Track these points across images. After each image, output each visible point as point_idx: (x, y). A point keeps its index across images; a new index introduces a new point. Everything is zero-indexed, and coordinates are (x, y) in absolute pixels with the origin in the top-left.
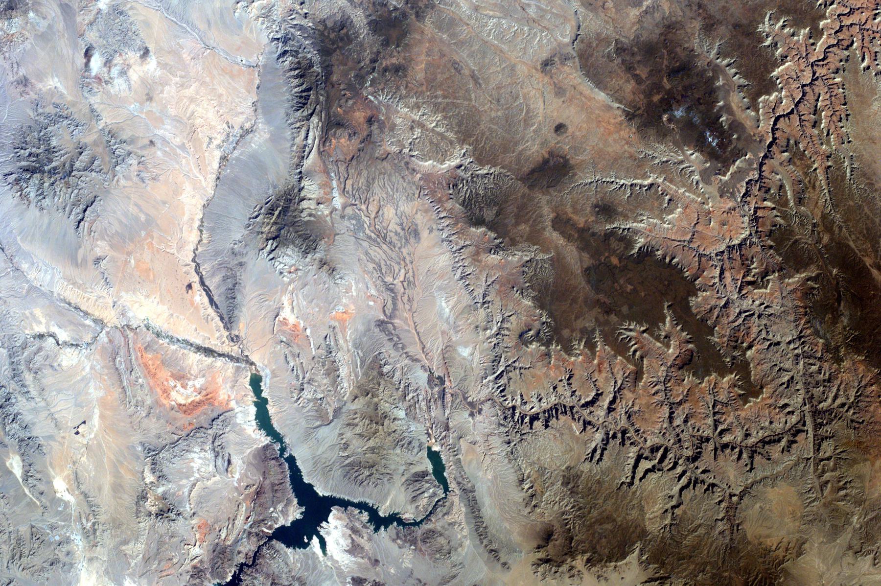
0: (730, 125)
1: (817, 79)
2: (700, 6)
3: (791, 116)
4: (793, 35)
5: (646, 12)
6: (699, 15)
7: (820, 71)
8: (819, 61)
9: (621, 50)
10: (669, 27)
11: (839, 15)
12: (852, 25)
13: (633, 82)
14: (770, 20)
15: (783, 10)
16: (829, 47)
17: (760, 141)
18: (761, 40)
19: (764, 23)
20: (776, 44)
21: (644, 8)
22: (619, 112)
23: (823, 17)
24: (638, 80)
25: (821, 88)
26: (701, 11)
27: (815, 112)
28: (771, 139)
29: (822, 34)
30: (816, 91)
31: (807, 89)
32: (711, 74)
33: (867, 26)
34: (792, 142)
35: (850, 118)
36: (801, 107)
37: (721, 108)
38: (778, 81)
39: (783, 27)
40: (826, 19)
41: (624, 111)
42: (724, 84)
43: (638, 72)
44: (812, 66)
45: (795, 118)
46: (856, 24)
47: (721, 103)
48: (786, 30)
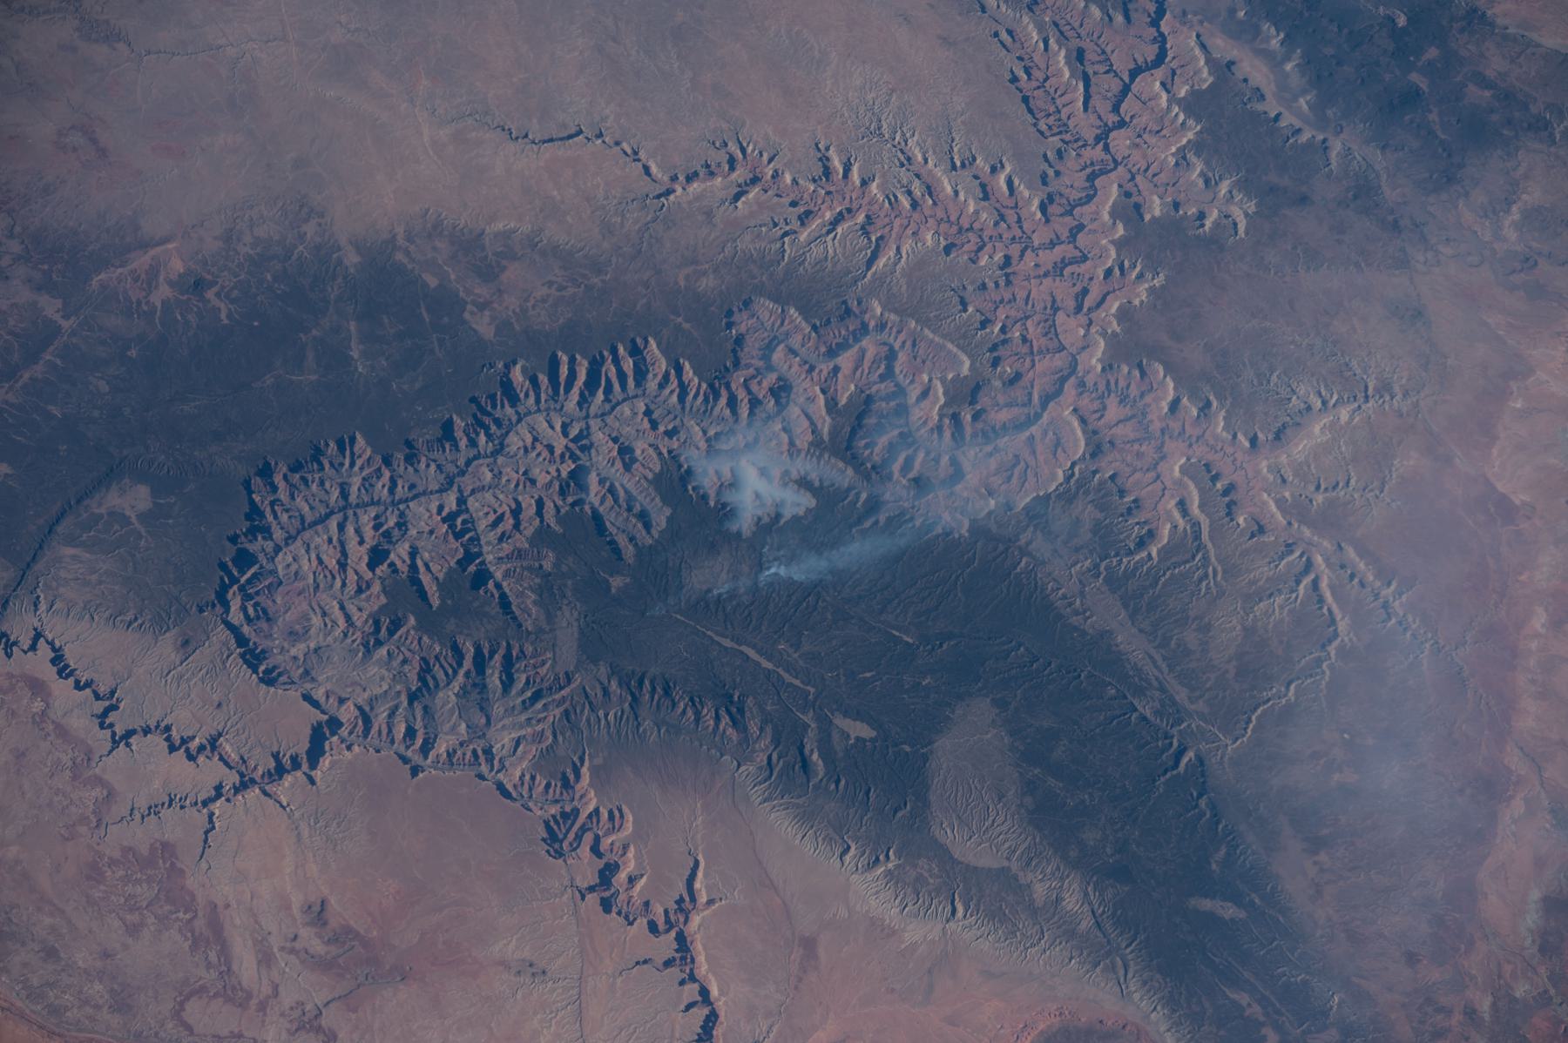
0: (1257, 31)
1: (1098, 139)
2: (1396, 227)
3: (1132, 66)
4: (1176, 205)
5: (1509, 203)
6: (1392, 212)
7: (1097, 153)
8: (1104, 172)
9: (1539, 127)
10: (1451, 180)
11: (1084, 258)
12: (1052, 245)
13: (1490, 73)
14: (1235, 224)
15: (1215, 243)
16: (1090, 198)
17: (1184, 13)
18: (1244, 185)
19: (1246, 215)
20: (1207, 182)
21: (1514, 208)
22: (1500, 21)
23: (1119, 245)
24: (1484, 82)
25: (1085, 125)
26: (1390, 218)
27: (1086, 80)
28: (1162, 23)
29: (1114, 214)
30: (1093, 119)
31: (1112, 119)
32: (1329, 113)
33: (1015, 250)
34: (1119, 19)
35: (1008, 76)
36: (1116, 86)
37: (1287, 58)
38: (1182, 117)
39: (1201, 216)
40: (1112, 242)
41: (1492, 24)
42: (1295, 98)
43: (1487, 94)
44: (1115, 161)
45: (1122, 65)
46: (1043, 247)
47: (1289, 67)
48: (1192, 211)
